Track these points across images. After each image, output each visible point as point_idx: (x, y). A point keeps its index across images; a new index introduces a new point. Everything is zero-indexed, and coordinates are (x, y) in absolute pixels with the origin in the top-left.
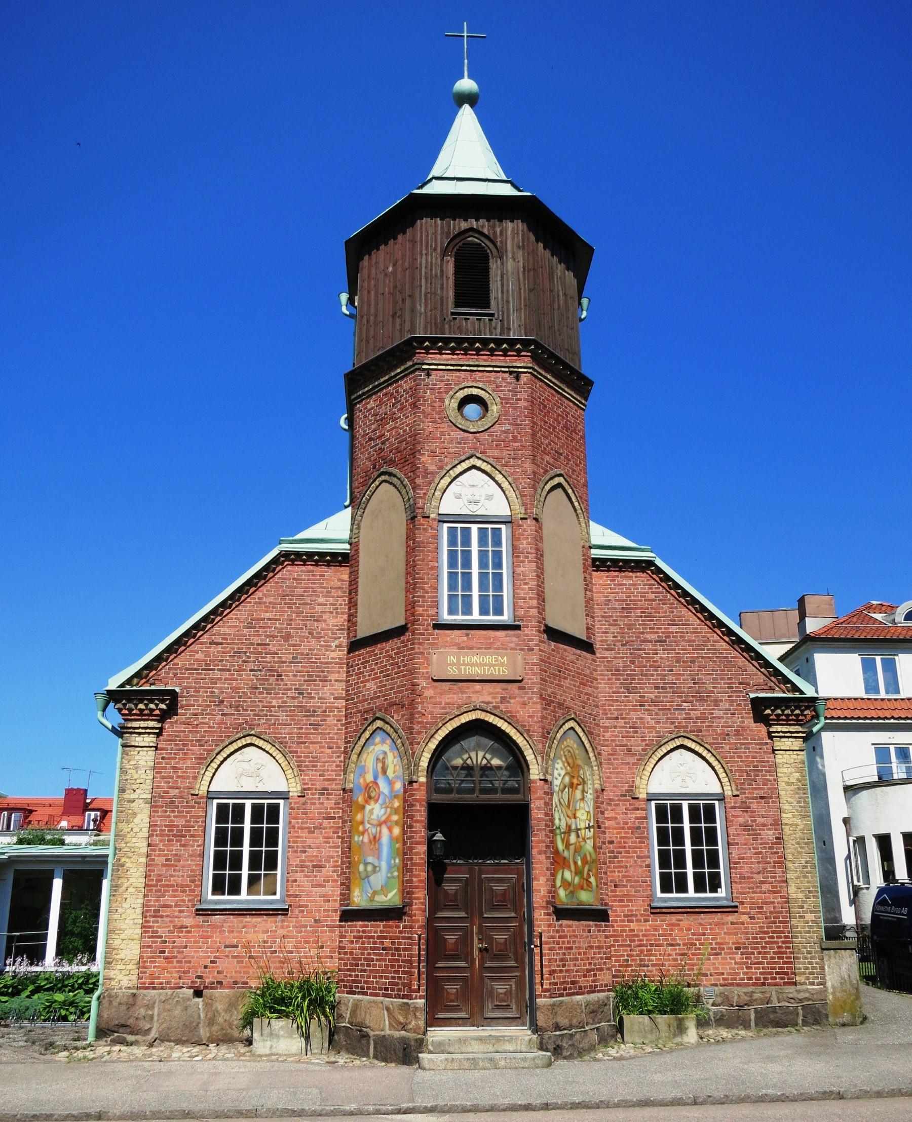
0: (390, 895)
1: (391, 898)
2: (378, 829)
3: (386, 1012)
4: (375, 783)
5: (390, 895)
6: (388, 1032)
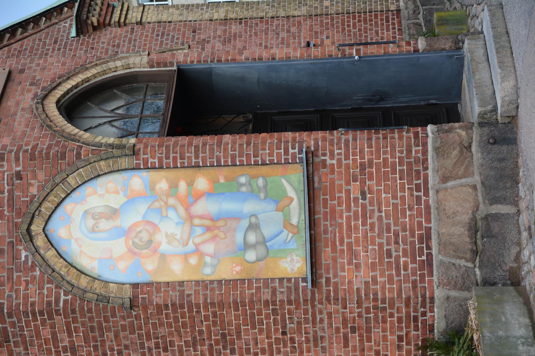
0: (291, 193)
1: (291, 184)
2: (197, 221)
3: (450, 184)
4: (126, 233)
5: (291, 193)
6: (477, 179)
